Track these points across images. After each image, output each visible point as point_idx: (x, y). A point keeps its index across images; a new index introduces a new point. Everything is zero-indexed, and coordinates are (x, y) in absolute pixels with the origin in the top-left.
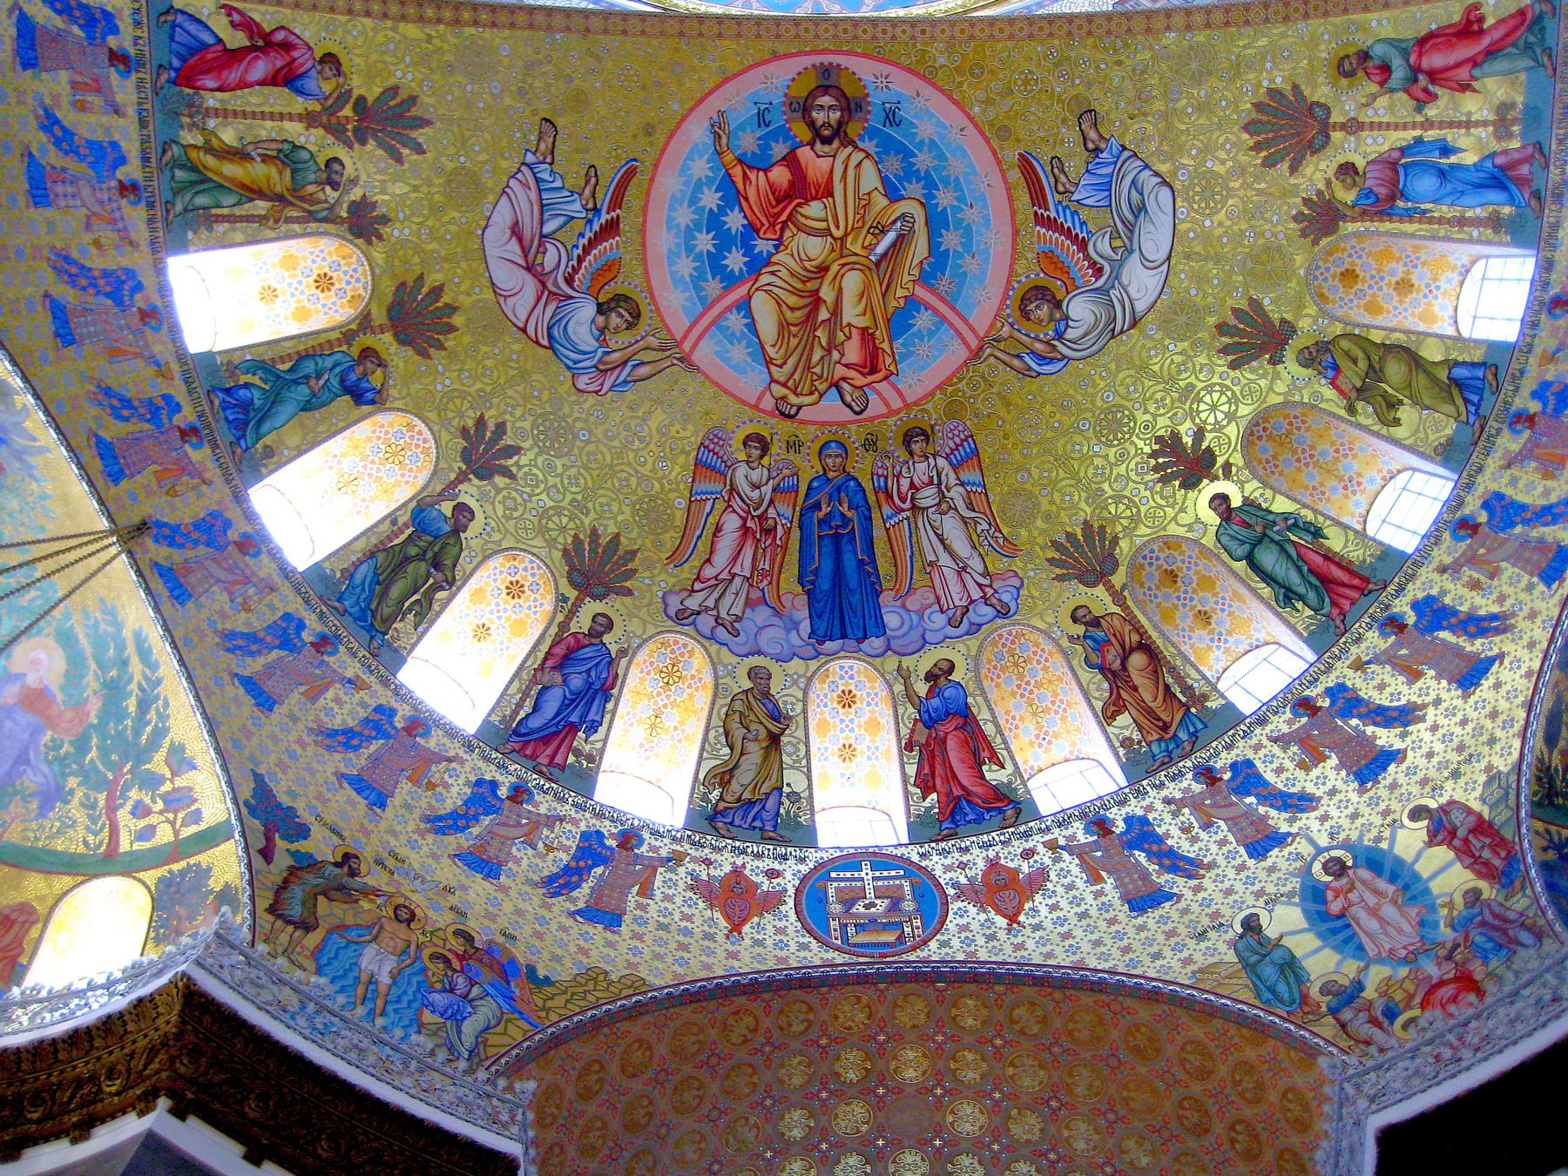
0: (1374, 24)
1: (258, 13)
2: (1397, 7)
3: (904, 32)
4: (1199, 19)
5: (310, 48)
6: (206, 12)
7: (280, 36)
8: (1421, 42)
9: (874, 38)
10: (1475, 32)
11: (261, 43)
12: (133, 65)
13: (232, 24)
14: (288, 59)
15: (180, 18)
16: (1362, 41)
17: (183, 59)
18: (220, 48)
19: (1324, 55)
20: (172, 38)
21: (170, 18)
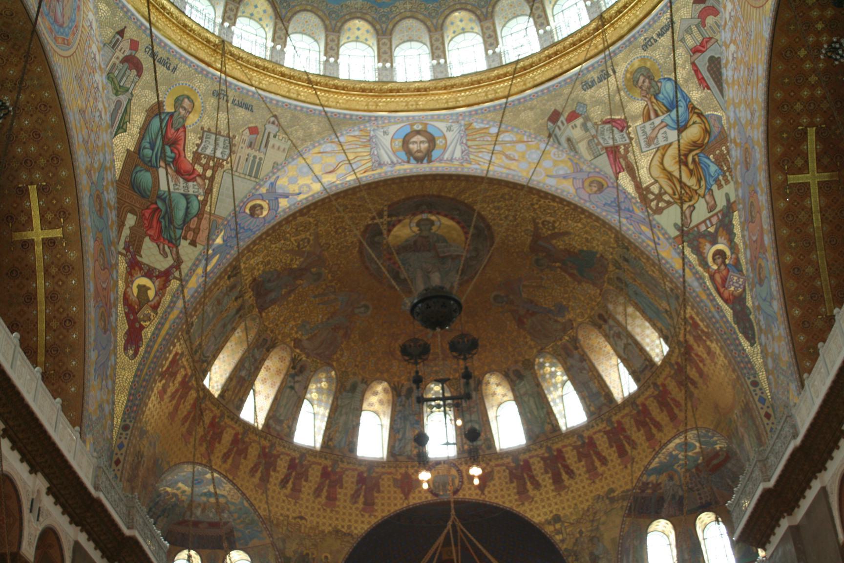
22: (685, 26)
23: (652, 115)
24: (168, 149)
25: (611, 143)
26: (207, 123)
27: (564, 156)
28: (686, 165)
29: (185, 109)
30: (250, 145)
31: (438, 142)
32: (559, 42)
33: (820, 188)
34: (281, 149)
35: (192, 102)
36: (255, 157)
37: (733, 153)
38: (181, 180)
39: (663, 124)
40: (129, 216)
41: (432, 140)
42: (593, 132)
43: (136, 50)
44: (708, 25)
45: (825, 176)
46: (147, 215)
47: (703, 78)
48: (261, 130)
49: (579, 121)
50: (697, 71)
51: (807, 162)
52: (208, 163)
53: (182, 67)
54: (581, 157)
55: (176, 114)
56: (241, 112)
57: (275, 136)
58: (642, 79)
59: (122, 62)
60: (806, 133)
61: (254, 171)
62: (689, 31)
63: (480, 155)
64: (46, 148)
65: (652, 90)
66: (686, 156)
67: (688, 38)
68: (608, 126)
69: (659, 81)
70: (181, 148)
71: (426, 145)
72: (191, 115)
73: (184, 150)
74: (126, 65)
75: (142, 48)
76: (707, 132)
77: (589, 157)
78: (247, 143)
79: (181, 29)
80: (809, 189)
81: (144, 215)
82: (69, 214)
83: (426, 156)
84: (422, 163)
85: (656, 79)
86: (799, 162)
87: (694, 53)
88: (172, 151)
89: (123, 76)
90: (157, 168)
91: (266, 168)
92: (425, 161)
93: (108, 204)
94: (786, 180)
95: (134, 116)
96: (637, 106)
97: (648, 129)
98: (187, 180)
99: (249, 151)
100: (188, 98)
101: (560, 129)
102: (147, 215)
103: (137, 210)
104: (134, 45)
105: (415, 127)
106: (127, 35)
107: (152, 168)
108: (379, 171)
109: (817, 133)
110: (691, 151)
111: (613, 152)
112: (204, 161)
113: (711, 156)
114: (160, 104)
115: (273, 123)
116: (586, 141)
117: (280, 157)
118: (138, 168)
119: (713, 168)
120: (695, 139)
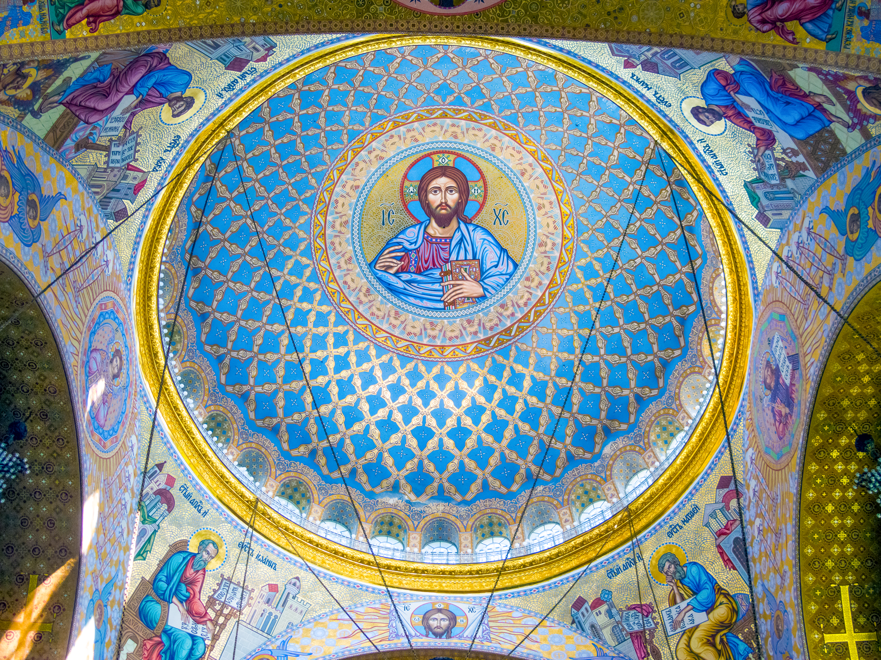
0: (144, 24)
1: (778, 40)
2: (133, 33)
3: (402, 25)
4: (237, 30)
5: (750, 21)
6: (808, 40)
7: (766, 27)
8: (118, 13)
9: (419, 22)
10: (92, 16)
11: (778, 24)
12: (856, 10)
13: (793, 33)
14: (763, 15)
15: (824, 37)
16: (149, 15)
17: (825, 14)
18: (803, 21)
19: (168, 8)
20: (830, 26)
21: (829, 36)
22: (709, 511)
23: (678, 599)
24: (183, 587)
25: (636, 628)
26: (227, 572)
27: (589, 642)
28: (713, 645)
29: (208, 553)
30: (268, 601)
31: (458, 620)
32: (586, 533)
33: (859, 649)
34: (299, 611)
35: (217, 549)
36: (271, 614)
37: (763, 628)
38: (191, 620)
39: (690, 607)
40: (130, 641)
41: (453, 618)
42: (618, 618)
43: (172, 486)
44: (732, 508)
45: (863, 637)
46: (148, 646)
47: (729, 559)
48: (281, 588)
49: (603, 608)
50: (722, 553)
51: (842, 621)
52: (221, 610)
53: (213, 512)
54: (605, 643)
55: (198, 556)
56: (265, 568)
57: (294, 598)
58: (667, 564)
59: (156, 493)
60: (839, 591)
61: (268, 626)
62: (713, 515)
63: (501, 635)
64: (57, 538)
65: (678, 574)
66: (713, 637)
67: (713, 522)
68: (632, 612)
69: (685, 566)
70: (197, 589)
71: (447, 622)
72: (213, 561)
73: (200, 593)
74: (159, 497)
75: (177, 485)
76: (734, 611)
77: (612, 643)
78: (265, 599)
79: (219, 479)
80: (847, 649)
81: (145, 645)
82: (64, 610)
83: (447, 632)
84: (440, 638)
85: (682, 564)
86: (835, 621)
87: (719, 536)
88: (187, 591)
89: (154, 507)
90: (169, 602)
91: (280, 627)
92: (444, 636)
93: (109, 620)
94: (823, 639)
95: (155, 547)
96: (663, 591)
97: (674, 613)
98: (198, 623)
99: (266, 606)
100: (214, 543)
101: (584, 616)
102: (148, 646)
103: (139, 638)
104: (171, 481)
105: (437, 606)
106: (167, 469)
107: (164, 599)
108: (396, 641)
109: (850, 592)
110: (718, 631)
111: (639, 638)
112: (218, 607)
113: (740, 636)
114: (186, 543)
115: (294, 584)
116: (609, 629)
117: (296, 619)
118: (150, 598)
119: (742, 647)
120: (722, 620)
